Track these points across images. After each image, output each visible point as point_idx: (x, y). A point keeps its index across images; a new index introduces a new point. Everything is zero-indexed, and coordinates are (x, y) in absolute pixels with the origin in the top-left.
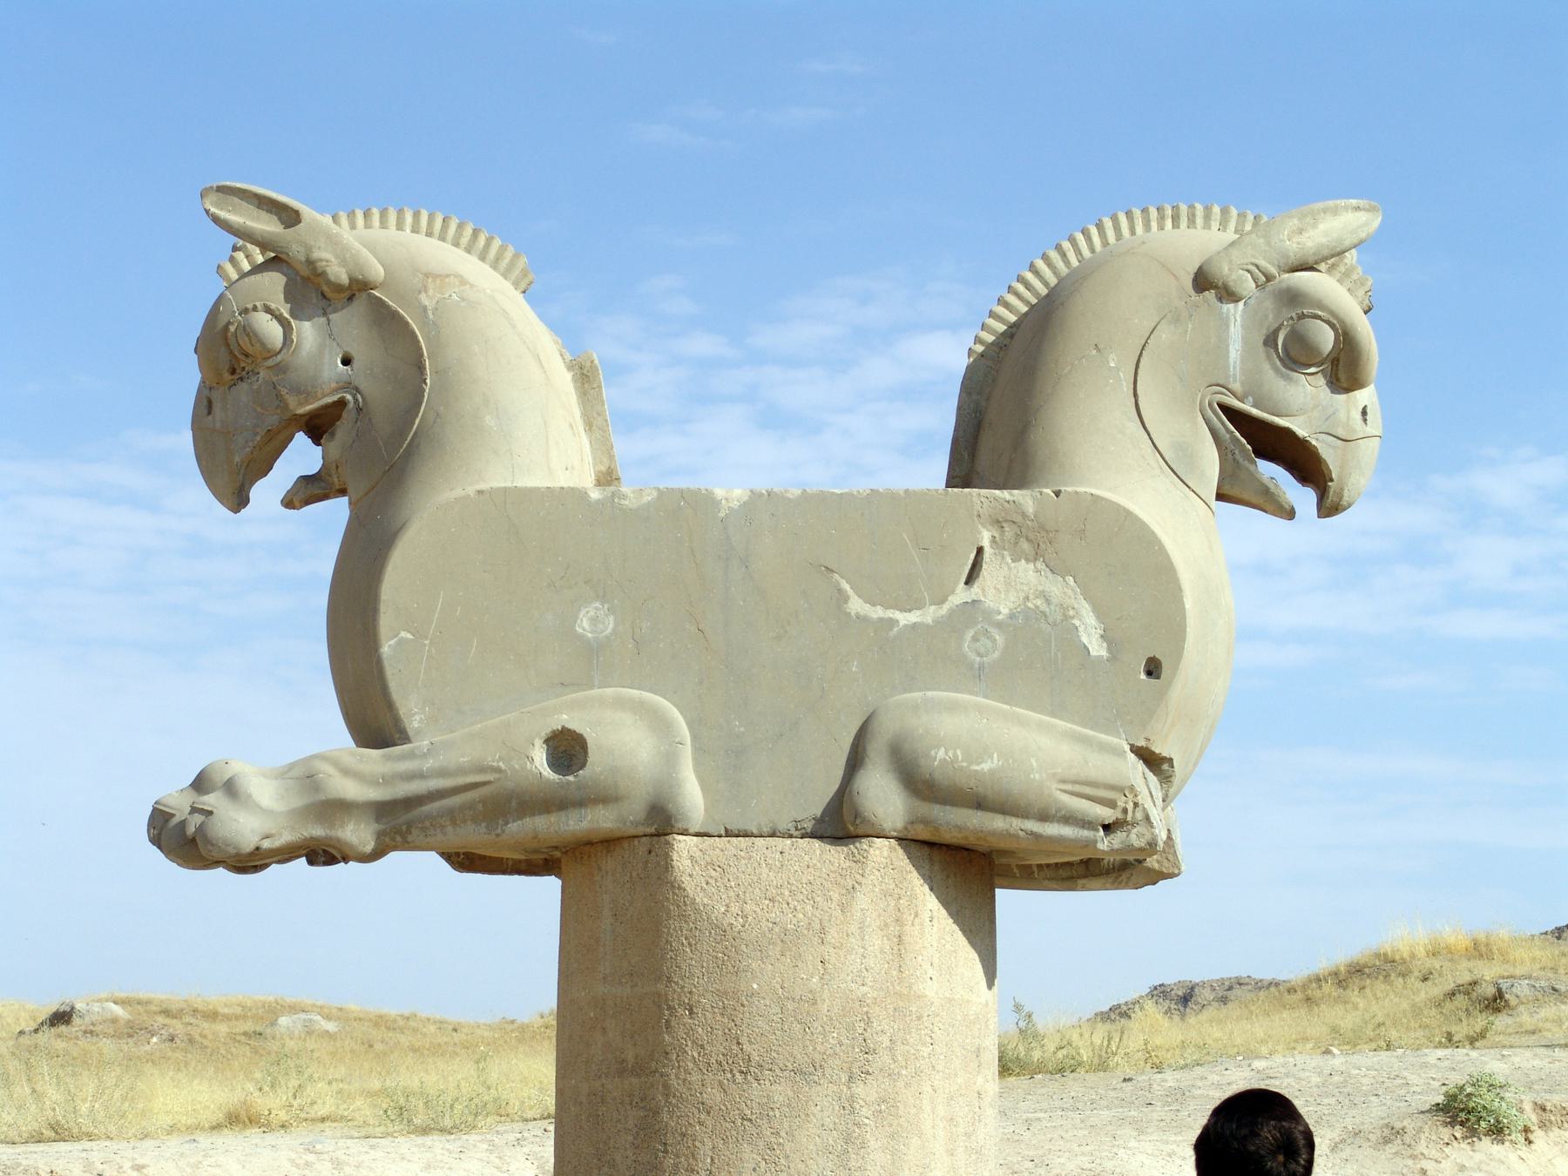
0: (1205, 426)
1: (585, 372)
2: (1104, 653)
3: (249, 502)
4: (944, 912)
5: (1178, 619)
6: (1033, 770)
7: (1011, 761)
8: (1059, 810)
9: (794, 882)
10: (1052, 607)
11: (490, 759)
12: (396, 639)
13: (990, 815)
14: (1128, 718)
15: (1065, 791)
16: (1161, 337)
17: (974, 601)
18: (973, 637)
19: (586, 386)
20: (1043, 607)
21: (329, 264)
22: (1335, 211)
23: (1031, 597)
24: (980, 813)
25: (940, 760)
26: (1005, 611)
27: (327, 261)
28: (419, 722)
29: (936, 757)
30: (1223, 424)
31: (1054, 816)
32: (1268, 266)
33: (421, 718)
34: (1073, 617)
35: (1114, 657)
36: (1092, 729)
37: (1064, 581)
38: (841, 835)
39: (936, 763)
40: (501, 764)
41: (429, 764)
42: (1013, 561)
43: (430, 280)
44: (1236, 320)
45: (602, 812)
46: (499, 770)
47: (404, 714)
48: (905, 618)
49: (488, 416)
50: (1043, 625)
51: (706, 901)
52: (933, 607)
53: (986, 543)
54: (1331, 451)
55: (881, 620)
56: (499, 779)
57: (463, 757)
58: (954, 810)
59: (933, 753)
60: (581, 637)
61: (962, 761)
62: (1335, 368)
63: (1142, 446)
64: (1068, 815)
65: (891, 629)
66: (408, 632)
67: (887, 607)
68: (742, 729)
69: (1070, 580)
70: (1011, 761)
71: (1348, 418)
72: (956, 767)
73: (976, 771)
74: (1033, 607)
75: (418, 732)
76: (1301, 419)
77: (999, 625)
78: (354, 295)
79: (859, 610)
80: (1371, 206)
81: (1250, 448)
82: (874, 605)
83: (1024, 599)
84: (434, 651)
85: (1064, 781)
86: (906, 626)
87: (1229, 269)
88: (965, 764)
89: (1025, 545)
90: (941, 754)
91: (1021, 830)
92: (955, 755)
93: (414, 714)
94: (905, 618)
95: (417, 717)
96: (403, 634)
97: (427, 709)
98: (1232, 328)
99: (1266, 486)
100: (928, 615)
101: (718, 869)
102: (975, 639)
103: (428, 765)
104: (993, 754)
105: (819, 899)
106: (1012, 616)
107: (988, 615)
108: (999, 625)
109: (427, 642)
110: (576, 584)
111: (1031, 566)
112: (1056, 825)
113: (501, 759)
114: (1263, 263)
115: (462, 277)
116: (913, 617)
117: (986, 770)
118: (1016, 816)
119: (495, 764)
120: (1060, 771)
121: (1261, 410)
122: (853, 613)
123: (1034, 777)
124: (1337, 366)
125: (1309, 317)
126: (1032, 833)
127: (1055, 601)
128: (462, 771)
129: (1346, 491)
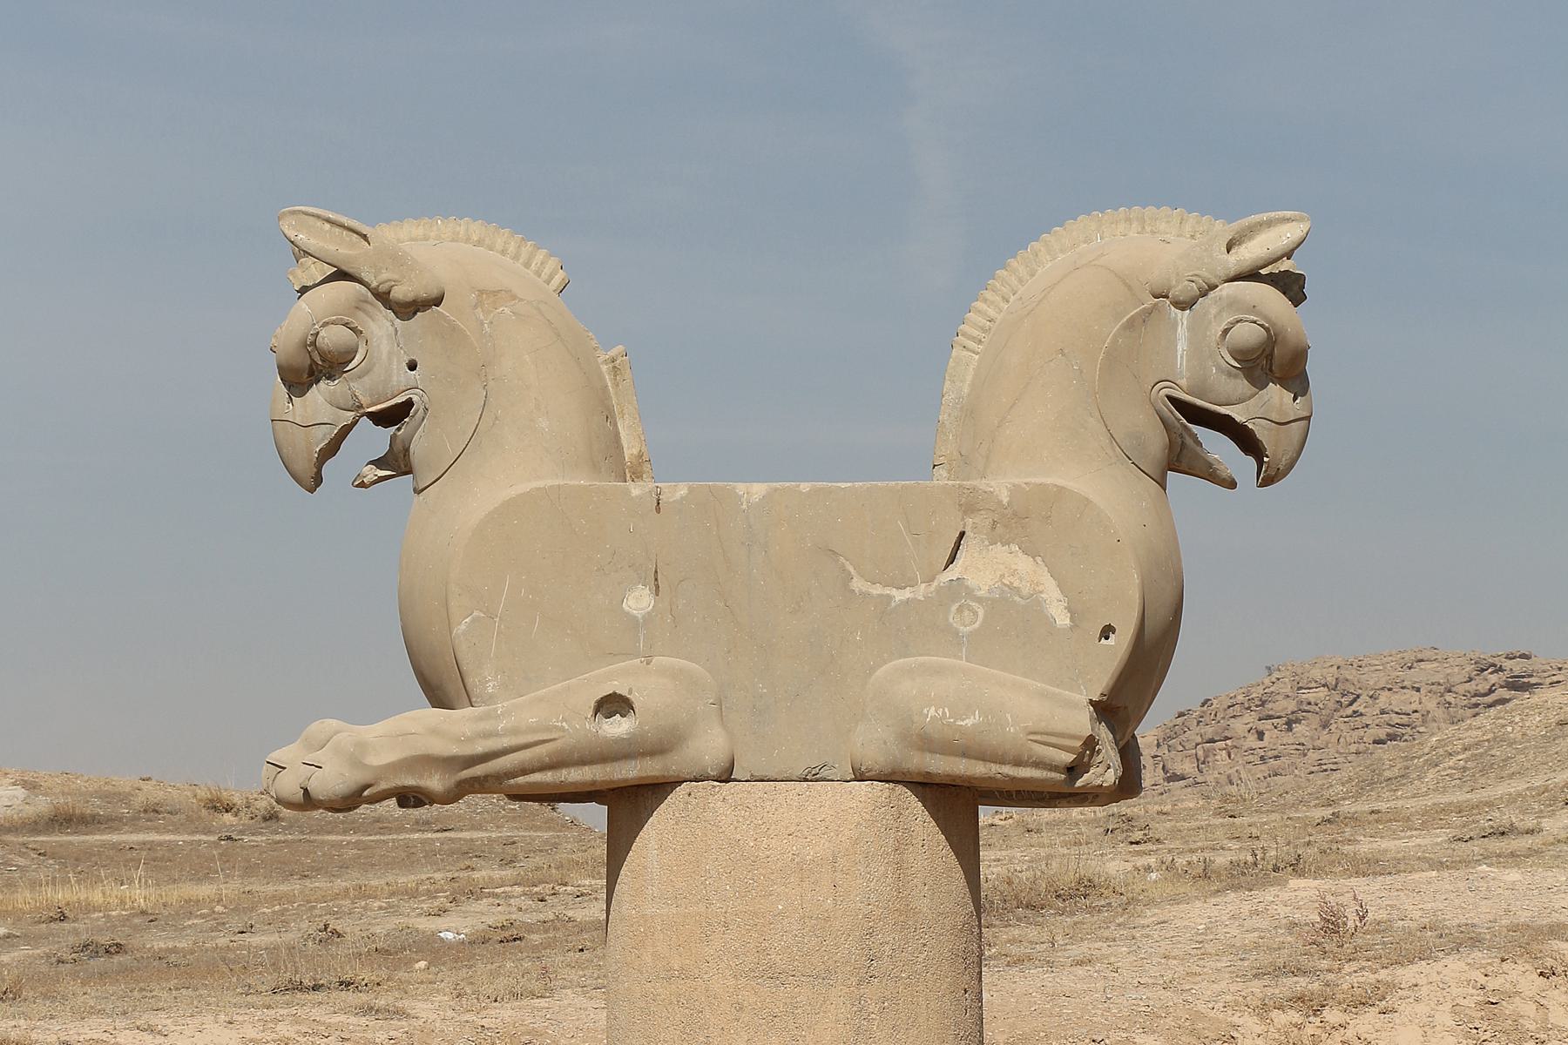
2: (1068, 622)
8: (1030, 757)
15: (1036, 741)
18: (957, 609)
22: (1270, 224)
31: (1027, 761)
33: (494, 685)
40: (564, 724)
44: (1182, 324)
46: (562, 729)
48: (900, 596)
50: (1017, 598)
59: (925, 711)
65: (889, 603)
69: (1039, 559)
77: (979, 600)
92: (944, 713)
94: (900, 596)
102: (960, 610)
106: (990, 591)
107: (970, 593)
108: (979, 600)
109: (497, 619)
112: (1028, 769)
116: (906, 594)
128: (534, 730)
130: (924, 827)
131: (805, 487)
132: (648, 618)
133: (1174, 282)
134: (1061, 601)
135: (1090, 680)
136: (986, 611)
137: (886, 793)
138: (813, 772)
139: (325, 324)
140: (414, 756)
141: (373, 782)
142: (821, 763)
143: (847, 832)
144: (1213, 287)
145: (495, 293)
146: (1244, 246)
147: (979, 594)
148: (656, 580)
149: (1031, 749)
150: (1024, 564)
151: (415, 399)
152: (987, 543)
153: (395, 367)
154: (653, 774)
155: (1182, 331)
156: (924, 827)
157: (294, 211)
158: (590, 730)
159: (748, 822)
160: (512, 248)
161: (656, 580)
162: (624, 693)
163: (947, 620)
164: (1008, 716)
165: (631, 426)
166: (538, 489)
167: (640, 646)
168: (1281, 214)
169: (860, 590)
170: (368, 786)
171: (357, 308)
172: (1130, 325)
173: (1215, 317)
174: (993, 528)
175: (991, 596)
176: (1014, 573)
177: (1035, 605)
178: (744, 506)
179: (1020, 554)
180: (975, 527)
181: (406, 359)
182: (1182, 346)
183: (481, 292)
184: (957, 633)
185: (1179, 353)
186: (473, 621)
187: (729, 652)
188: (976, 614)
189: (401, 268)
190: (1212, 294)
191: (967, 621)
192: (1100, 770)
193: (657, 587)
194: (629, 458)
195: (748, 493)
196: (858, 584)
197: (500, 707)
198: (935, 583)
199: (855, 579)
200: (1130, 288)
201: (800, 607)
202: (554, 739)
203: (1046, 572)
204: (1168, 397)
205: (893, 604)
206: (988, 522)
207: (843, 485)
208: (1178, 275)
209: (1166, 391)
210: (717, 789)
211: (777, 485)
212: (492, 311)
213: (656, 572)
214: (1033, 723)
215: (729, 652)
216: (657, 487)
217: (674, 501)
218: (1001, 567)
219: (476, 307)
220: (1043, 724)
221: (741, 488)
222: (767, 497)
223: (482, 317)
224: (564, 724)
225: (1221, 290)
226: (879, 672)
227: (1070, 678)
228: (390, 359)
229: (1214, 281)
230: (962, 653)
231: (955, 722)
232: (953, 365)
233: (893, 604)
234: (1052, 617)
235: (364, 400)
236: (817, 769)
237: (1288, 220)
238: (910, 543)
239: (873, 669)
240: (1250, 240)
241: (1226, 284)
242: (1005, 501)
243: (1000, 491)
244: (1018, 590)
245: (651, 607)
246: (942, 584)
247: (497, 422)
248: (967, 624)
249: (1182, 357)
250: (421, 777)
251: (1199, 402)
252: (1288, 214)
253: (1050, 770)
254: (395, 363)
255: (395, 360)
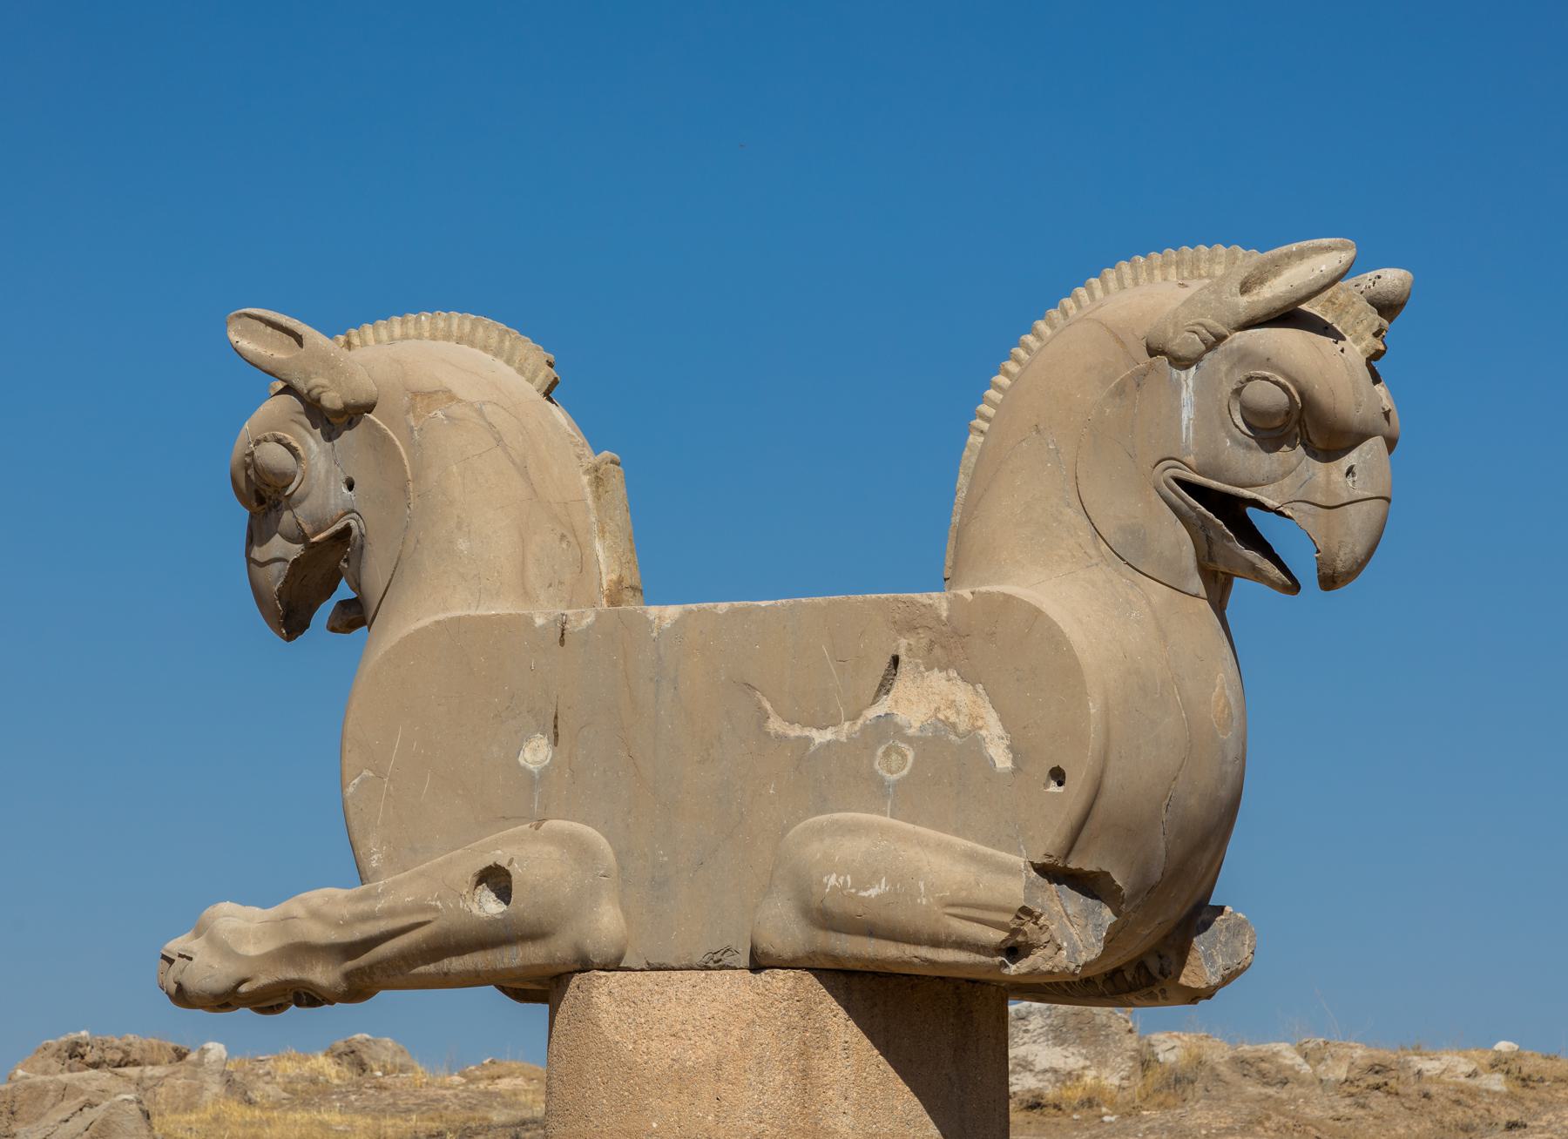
0: (1164, 503)
1: (599, 475)
2: (1009, 764)
3: (307, 626)
4: (867, 1042)
5: (1083, 725)
6: (921, 894)
7: (898, 886)
8: (948, 936)
9: (699, 1018)
10: (961, 717)
11: (429, 898)
12: (358, 778)
13: (883, 942)
14: (1031, 833)
15: (955, 916)
16: (1105, 412)
17: (887, 714)
18: (884, 752)
19: (600, 489)
20: (953, 719)
21: (325, 389)
22: (1301, 255)
23: (943, 707)
24: (873, 941)
25: (831, 887)
26: (918, 725)
27: (323, 387)
28: (377, 862)
29: (827, 884)
30: (1183, 499)
31: (946, 941)
32: (1217, 324)
33: (379, 858)
34: (980, 728)
35: (1017, 768)
36: (993, 846)
37: (975, 689)
38: (785, 966)
39: (827, 890)
40: (438, 903)
41: (380, 905)
42: (927, 670)
43: (418, 399)
44: (1187, 386)
45: (532, 949)
46: (436, 909)
47: (364, 854)
48: (820, 737)
49: (461, 540)
50: (952, 737)
51: (617, 1038)
52: (847, 724)
53: (902, 653)
54: (1310, 519)
55: (798, 738)
56: (436, 918)
57: (409, 897)
58: (849, 937)
59: (825, 880)
60: (524, 769)
61: (851, 888)
62: (1304, 430)
63: (1080, 533)
64: (959, 940)
65: (807, 748)
66: (372, 770)
67: (805, 725)
68: (666, 859)
69: (980, 687)
70: (898, 886)
71: (1328, 482)
72: (845, 894)
73: (864, 897)
74: (943, 718)
75: (376, 871)
76: (1271, 487)
77: (910, 740)
78: (352, 419)
79: (778, 728)
80: (1343, 245)
81: (1221, 523)
82: (792, 723)
83: (935, 710)
84: (391, 788)
85: (953, 905)
86: (820, 743)
87: (1174, 333)
88: (853, 891)
89: (938, 651)
90: (832, 880)
91: (916, 957)
92: (845, 882)
93: (373, 854)
94: (820, 737)
95: (375, 857)
96: (366, 773)
97: (385, 847)
98: (1184, 391)
99: (1251, 562)
100: (844, 731)
101: (633, 1005)
102: (886, 754)
103: (379, 906)
104: (882, 878)
105: (720, 1034)
106: (922, 729)
107: (899, 731)
108: (910, 740)
109: (386, 780)
110: (520, 713)
111: (944, 674)
112: (950, 951)
113: (439, 898)
114: (1209, 321)
115: (450, 391)
116: (828, 735)
117: (873, 896)
118: (908, 942)
119: (433, 903)
120: (948, 894)
121: (1223, 483)
122: (772, 732)
123: (921, 902)
124: (1305, 426)
125: (1257, 378)
126: (927, 960)
127: (965, 710)
128: (408, 911)
129: (1338, 562)
130: (847, 1026)
131: (723, 607)
132: (545, 772)
133: (1171, 335)
134: (1003, 738)
135: (1033, 838)
136: (916, 755)
137: (790, 984)
138: (715, 959)
139: (258, 442)
140: (291, 945)
141: (249, 976)
142: (724, 945)
143: (736, 1032)
144: (1220, 338)
145: (430, 394)
146: (1268, 284)
147: (910, 732)
148: (556, 727)
149: (949, 926)
150: (962, 694)
151: (353, 523)
152: (922, 668)
153: (332, 487)
154: (537, 962)
155: (1187, 395)
156: (847, 1026)
157: (240, 314)
158: (463, 910)
159: (630, 1021)
160: (494, 341)
161: (556, 727)
162: (503, 863)
163: (872, 765)
164: (921, 885)
165: (612, 546)
166: (438, 622)
167: (534, 807)
168: (1317, 242)
169: (776, 733)
170: (244, 981)
171: (292, 420)
172: (1120, 391)
173: (1226, 375)
174: (930, 650)
175: (923, 735)
176: (952, 704)
177: (973, 742)
178: (655, 634)
179: (959, 682)
180: (909, 649)
181: (343, 477)
182: (1187, 414)
183: (415, 394)
184: (882, 780)
185: (1184, 423)
186: (362, 781)
187: (629, 812)
188: (904, 757)
189: (331, 372)
190: (1221, 347)
191: (894, 766)
192: (1048, 951)
193: (556, 735)
194: (609, 585)
195: (660, 618)
196: (775, 725)
197: (380, 884)
198: (860, 722)
199: (772, 719)
200: (1122, 344)
201: (709, 755)
202: (429, 922)
203: (987, 702)
204: (1179, 481)
205: (812, 748)
206: (924, 642)
207: (763, 604)
208: (1176, 324)
209: (1171, 472)
210: (603, 981)
211: (693, 606)
212: (424, 416)
213: (556, 717)
214: (951, 892)
215: (629, 812)
216: (563, 615)
217: (579, 631)
218: (937, 697)
219: (408, 412)
220: (964, 894)
221: (653, 611)
222: (679, 623)
223: (413, 424)
224: (438, 903)
225: (1231, 341)
226: (792, 832)
227: (1008, 836)
228: (327, 478)
229: (1223, 330)
230: (887, 806)
231: (857, 892)
232: (969, 454)
233: (812, 748)
234: (992, 759)
235: (308, 529)
236: (719, 954)
237: (1329, 249)
238: (834, 672)
239: (786, 830)
240: (1275, 276)
241: (1238, 334)
242: (944, 614)
243: (940, 603)
244: (954, 725)
245: (548, 761)
246: (868, 722)
247: (418, 546)
248: (896, 768)
249: (1187, 428)
250: (302, 969)
251: (1214, 484)
252: (1326, 241)
253: (978, 952)
254: (332, 483)
255: (333, 479)
